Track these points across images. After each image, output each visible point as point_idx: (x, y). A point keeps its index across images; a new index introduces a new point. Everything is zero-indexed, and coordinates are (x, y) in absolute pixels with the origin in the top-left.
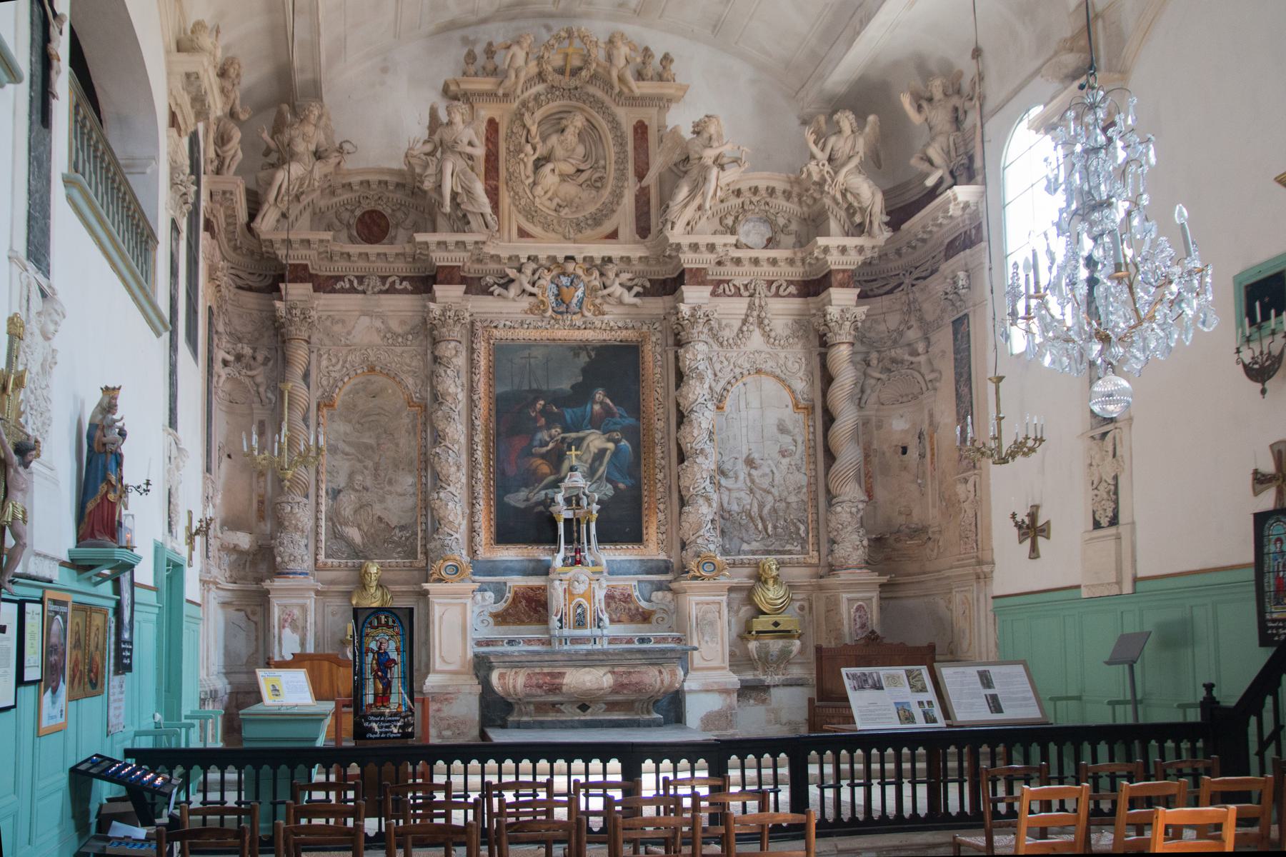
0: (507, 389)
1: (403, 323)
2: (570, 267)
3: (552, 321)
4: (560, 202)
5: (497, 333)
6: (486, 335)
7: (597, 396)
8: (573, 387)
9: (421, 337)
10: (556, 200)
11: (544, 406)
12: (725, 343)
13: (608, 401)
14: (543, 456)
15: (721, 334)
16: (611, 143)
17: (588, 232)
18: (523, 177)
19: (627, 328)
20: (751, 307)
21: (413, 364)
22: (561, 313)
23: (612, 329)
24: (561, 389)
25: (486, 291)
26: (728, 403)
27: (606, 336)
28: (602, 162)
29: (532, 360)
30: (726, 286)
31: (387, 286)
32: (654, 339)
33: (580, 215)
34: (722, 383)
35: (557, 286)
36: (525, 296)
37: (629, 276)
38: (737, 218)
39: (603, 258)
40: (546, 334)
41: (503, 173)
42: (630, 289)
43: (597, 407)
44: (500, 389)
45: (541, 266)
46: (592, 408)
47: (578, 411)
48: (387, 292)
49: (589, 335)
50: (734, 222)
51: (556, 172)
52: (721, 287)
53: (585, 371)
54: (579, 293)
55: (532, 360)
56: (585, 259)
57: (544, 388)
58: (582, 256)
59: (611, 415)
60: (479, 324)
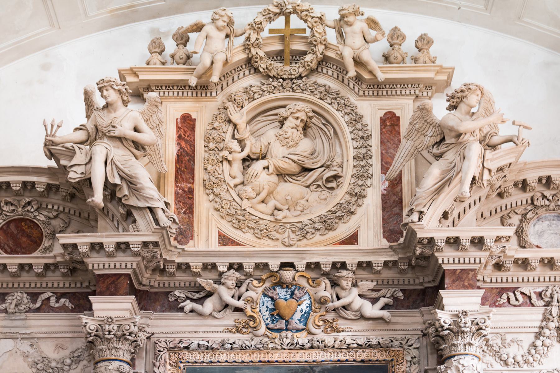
2: (288, 275)
4: (279, 206)
9: (85, 362)
10: (272, 203)
15: (504, 351)
16: (349, 136)
17: (318, 237)
18: (228, 179)
19: (370, 346)
20: (545, 319)
22: (280, 330)
23: (349, 348)
28: (338, 160)
30: (511, 295)
33: (305, 219)
35: (272, 299)
36: (228, 311)
37: (372, 285)
38: (524, 216)
39: (334, 265)
40: (256, 357)
41: (200, 174)
42: (374, 301)
45: (249, 275)
48: (38, 310)
50: (521, 221)
51: (271, 169)
52: (505, 296)
56: (308, 266)
58: (305, 262)
60: (163, 344)
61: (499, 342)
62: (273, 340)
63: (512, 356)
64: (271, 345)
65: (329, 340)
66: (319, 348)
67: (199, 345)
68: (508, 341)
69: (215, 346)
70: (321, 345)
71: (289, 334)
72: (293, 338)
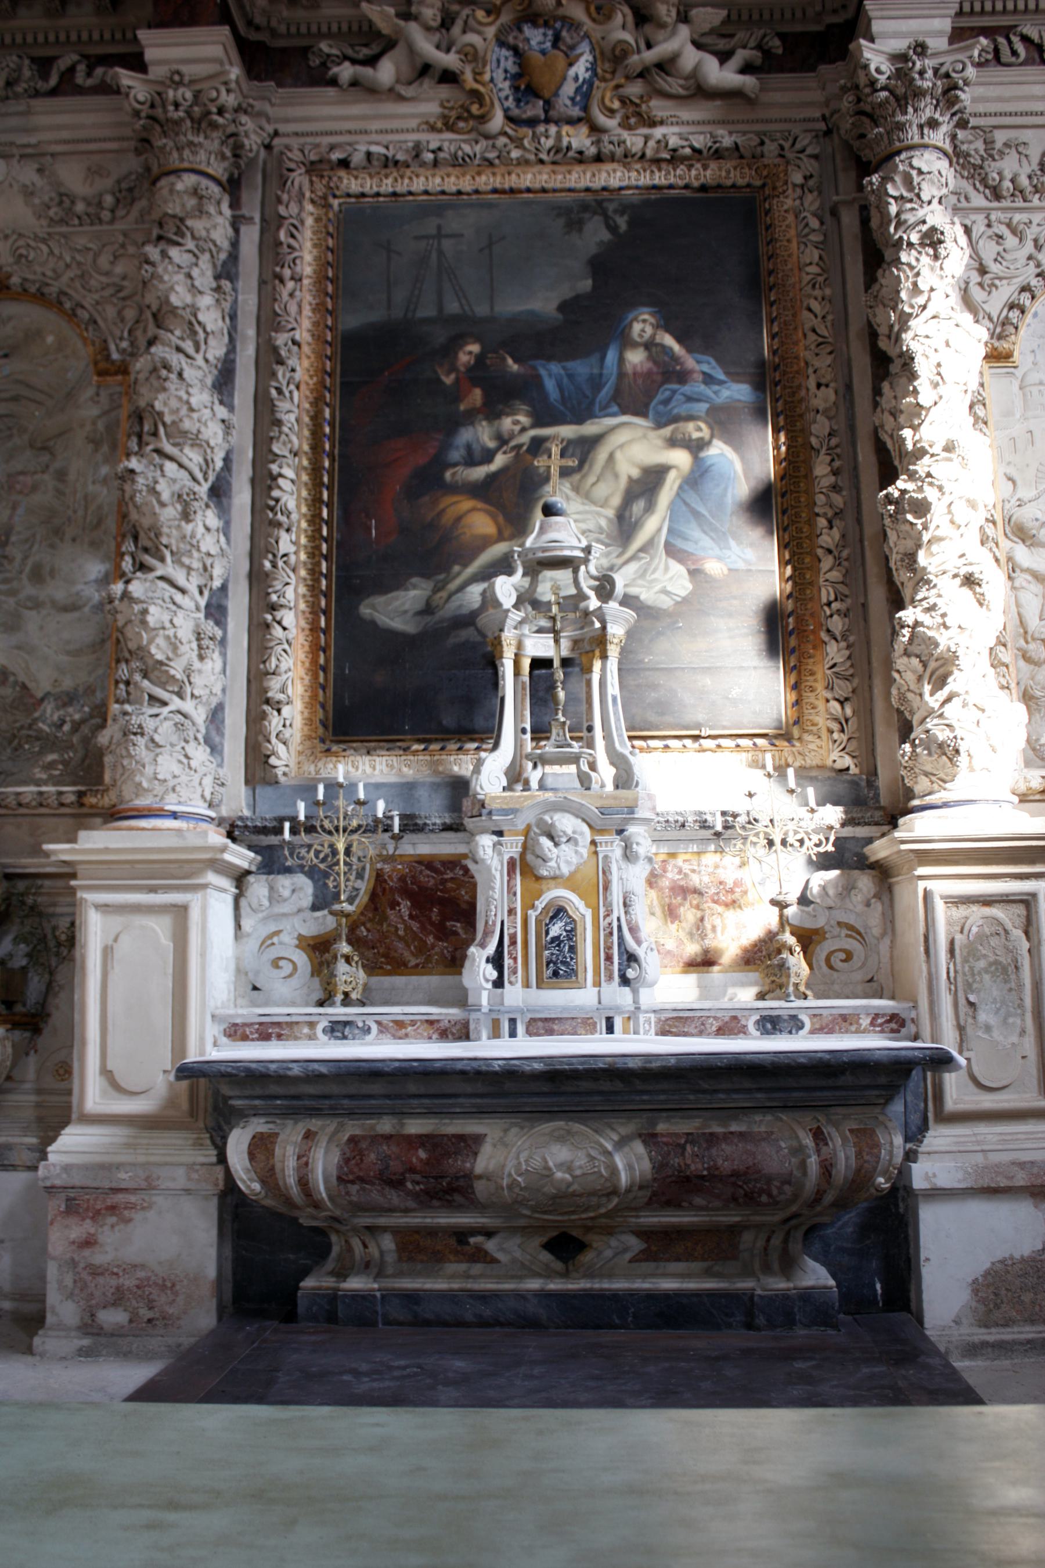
0: (376, 316)
1: (94, 172)
3: (502, 140)
5: (352, 184)
6: (320, 187)
7: (637, 327)
8: (563, 307)
11: (480, 358)
12: (1007, 184)
13: (669, 341)
14: (483, 491)
19: (718, 154)
21: (119, 269)
24: (532, 313)
25: (322, 78)
26: (1022, 344)
27: (659, 178)
29: (447, 244)
31: (53, 81)
32: (797, 178)
34: (1006, 292)
40: (486, 181)
43: (636, 358)
44: (352, 321)
46: (621, 360)
47: (582, 368)
49: (612, 176)
53: (598, 266)
54: (581, 69)
55: (447, 244)
57: (481, 310)
59: (682, 377)
60: (296, 155)
61: (980, 145)
62: (518, 143)
63: (1008, 175)
64: (515, 154)
65: (634, 141)
66: (612, 158)
67: (369, 155)
68: (998, 145)
69: (400, 157)
70: (619, 151)
71: (553, 129)
72: (559, 137)
